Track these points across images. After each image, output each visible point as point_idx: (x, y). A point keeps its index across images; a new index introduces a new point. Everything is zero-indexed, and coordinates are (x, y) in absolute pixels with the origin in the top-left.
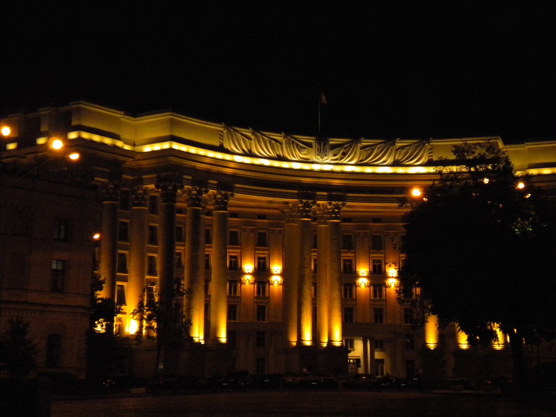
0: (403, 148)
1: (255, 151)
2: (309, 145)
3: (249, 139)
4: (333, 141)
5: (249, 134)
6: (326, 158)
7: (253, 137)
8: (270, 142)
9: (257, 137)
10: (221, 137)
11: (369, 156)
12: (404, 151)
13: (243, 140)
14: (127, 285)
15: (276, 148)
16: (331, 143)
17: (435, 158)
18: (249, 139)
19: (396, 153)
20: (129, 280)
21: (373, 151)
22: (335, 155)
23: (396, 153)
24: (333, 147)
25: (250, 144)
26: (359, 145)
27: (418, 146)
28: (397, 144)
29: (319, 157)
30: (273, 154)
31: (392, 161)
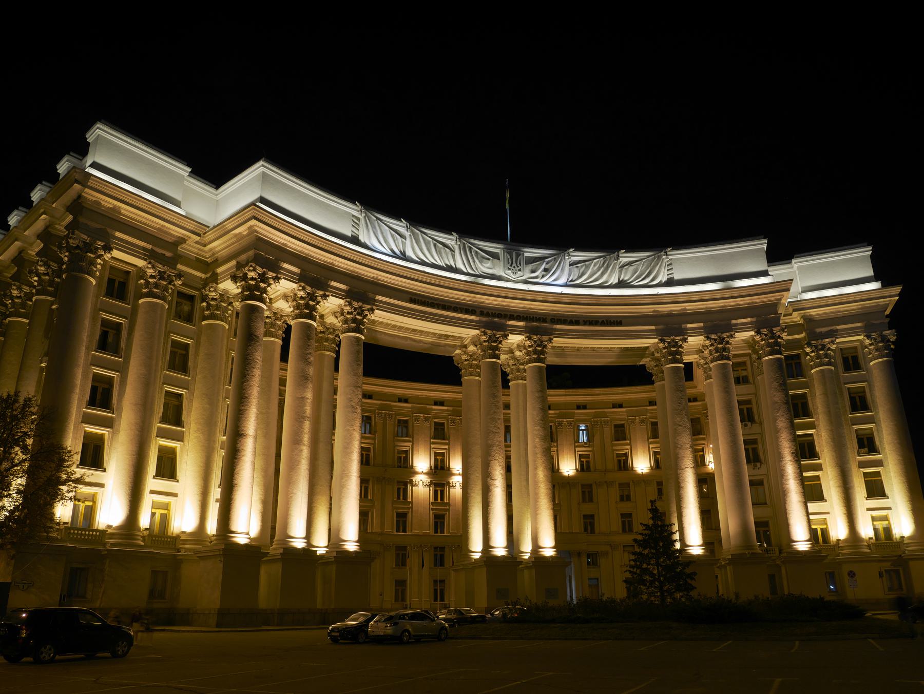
0: (630, 264)
1: (410, 253)
2: (495, 256)
3: (402, 236)
4: (531, 252)
5: (403, 230)
6: (520, 273)
7: (407, 234)
8: (435, 245)
9: (412, 232)
10: (356, 225)
11: (583, 274)
12: (631, 268)
13: (392, 236)
14: (182, 447)
15: (444, 255)
16: (526, 255)
17: (677, 276)
18: (402, 236)
19: (621, 272)
20: (186, 439)
21: (587, 267)
22: (533, 272)
23: (621, 272)
24: (531, 260)
25: (404, 244)
26: (568, 259)
27: (653, 260)
28: (621, 259)
29: (509, 272)
30: (439, 263)
31: (616, 281)
